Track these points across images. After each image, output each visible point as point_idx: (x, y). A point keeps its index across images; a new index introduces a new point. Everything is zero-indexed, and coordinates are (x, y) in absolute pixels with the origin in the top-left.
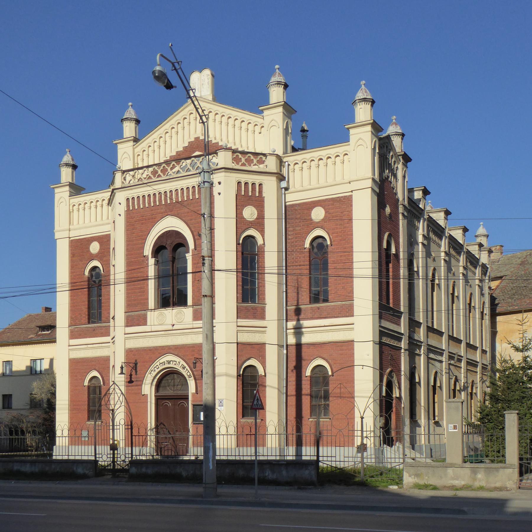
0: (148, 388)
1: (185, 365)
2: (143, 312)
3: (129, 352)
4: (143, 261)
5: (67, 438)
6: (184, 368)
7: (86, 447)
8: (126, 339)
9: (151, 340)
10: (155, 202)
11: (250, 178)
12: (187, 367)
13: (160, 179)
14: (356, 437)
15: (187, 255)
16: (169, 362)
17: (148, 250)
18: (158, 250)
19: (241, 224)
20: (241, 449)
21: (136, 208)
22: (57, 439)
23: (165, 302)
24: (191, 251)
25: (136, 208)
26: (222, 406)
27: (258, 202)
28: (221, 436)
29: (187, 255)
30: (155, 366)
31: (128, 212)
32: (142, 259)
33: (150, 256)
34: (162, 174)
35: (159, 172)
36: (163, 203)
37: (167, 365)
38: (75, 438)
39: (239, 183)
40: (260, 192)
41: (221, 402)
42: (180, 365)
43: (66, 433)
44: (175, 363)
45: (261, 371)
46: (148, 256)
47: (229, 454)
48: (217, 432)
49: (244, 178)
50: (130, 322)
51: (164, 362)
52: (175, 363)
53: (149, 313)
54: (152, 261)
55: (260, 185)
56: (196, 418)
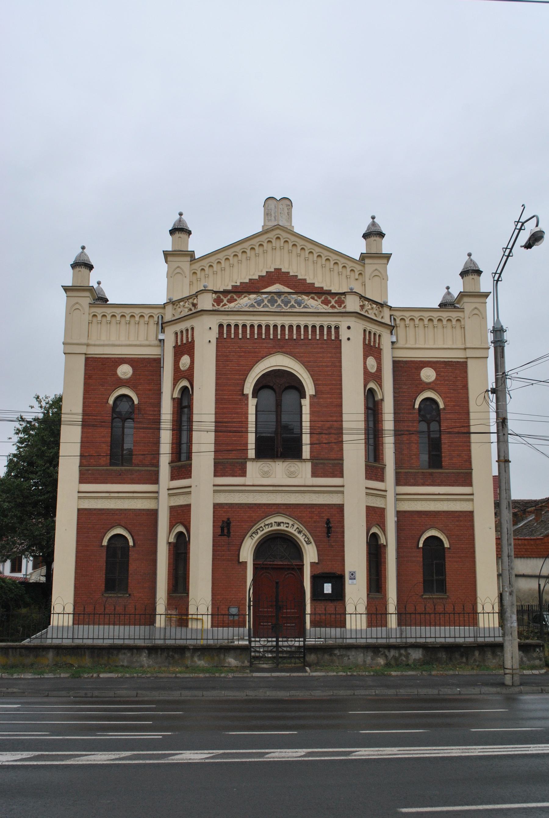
0: (247, 553)
1: (302, 528)
4: (240, 400)
5: (71, 616)
6: (300, 532)
8: (215, 491)
9: (251, 495)
10: (260, 333)
12: (305, 531)
14: (52, 615)
15: (303, 401)
16: (279, 524)
17: (248, 389)
19: (368, 376)
20: (374, 629)
21: (233, 336)
25: (248, 337)
26: (355, 579)
28: (486, 615)
29: (303, 401)
30: (258, 527)
31: (220, 339)
32: (240, 397)
33: (250, 396)
35: (279, 302)
36: (272, 337)
37: (275, 528)
38: (82, 615)
39: (365, 331)
41: (352, 574)
42: (295, 528)
44: (287, 525)
45: (382, 541)
46: (247, 395)
47: (379, 636)
51: (271, 523)
52: (287, 525)
53: (249, 465)
54: (252, 403)
55: (380, 336)
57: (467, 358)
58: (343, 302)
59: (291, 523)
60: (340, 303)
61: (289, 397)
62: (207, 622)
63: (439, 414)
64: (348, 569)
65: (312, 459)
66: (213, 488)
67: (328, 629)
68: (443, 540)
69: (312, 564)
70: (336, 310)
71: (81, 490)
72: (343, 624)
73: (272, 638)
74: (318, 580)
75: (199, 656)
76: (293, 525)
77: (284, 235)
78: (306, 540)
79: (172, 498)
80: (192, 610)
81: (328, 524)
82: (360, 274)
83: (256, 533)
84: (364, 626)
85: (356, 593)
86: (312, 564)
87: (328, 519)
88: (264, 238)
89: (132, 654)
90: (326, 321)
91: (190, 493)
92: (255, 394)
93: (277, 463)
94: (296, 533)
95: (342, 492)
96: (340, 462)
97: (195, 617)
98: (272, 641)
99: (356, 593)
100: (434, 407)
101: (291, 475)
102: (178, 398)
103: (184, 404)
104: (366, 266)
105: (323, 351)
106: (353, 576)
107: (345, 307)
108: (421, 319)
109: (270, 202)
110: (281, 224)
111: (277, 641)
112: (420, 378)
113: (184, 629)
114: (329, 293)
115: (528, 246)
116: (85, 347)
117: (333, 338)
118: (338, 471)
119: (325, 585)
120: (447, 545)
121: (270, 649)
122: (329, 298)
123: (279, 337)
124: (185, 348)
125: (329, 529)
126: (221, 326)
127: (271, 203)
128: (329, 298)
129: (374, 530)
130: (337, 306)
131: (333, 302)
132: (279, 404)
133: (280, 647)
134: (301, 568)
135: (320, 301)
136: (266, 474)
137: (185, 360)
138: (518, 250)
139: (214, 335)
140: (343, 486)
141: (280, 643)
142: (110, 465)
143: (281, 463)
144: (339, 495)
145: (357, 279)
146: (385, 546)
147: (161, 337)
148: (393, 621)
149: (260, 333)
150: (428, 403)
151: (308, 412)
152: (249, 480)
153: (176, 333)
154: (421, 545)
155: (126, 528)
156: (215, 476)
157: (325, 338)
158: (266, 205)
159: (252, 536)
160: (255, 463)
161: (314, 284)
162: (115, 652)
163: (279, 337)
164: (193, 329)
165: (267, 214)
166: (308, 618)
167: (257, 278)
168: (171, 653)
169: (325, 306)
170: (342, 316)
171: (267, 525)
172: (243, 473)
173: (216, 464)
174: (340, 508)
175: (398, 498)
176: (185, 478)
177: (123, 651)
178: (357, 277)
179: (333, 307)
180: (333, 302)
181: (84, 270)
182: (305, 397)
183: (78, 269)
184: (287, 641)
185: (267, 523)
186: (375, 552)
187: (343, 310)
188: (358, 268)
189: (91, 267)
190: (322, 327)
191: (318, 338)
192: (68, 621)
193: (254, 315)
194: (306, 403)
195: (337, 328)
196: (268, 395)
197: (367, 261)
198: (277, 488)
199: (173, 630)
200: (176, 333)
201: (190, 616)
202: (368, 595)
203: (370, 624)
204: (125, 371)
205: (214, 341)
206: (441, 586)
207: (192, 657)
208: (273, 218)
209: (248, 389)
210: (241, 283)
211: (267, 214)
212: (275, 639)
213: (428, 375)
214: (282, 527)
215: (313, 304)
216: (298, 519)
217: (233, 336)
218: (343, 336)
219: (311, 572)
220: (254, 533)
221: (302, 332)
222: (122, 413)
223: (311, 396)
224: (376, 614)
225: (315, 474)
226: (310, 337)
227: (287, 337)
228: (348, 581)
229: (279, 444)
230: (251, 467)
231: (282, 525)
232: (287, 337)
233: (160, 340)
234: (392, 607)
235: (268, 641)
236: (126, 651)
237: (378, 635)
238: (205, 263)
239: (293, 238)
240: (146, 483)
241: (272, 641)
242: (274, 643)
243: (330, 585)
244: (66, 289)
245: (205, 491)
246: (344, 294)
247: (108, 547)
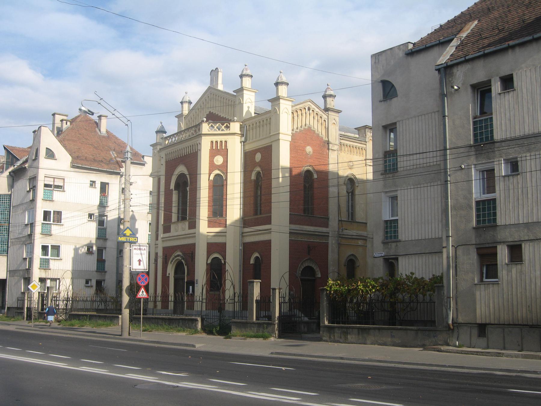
11: (219, 139)
17: (172, 186)
18: (177, 186)
27: (225, 153)
31: (166, 162)
39: (212, 142)
40: (226, 146)
45: (223, 262)
49: (214, 139)
55: (226, 142)
57: (272, 142)
83: (172, 261)
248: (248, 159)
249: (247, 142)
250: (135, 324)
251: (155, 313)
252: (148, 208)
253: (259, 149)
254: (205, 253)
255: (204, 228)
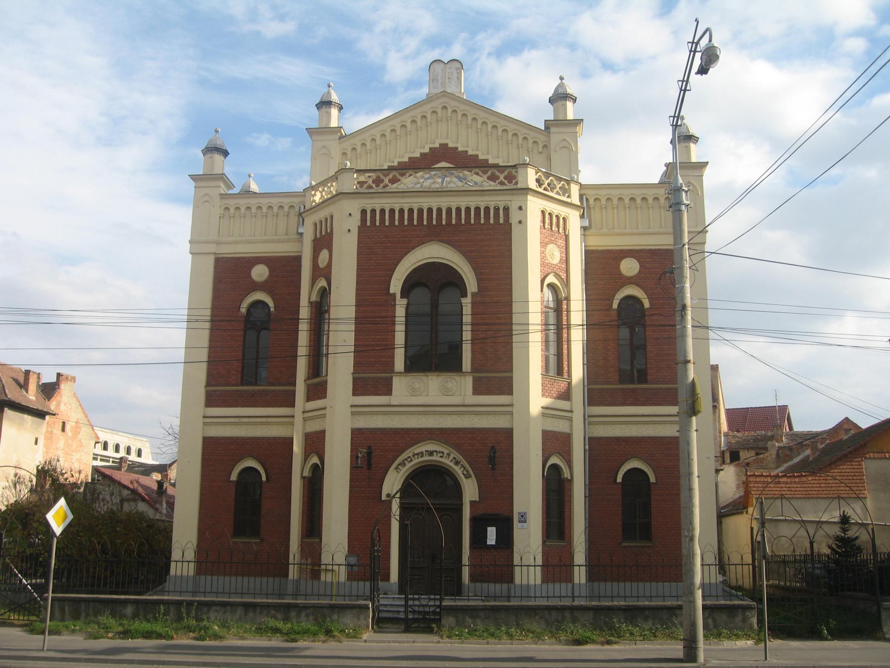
1: (460, 457)
2: (387, 375)
3: (357, 434)
5: (192, 565)
6: (457, 463)
7: (209, 578)
8: (353, 413)
10: (411, 218)
13: (371, 191)
15: (464, 300)
16: (431, 453)
17: (396, 286)
20: (551, 586)
21: (378, 224)
22: (173, 565)
23: (418, 363)
24: (469, 295)
26: (525, 522)
29: (464, 300)
33: (398, 295)
34: (374, 186)
39: (543, 212)
42: (451, 458)
43: (190, 555)
45: (566, 474)
46: (395, 294)
48: (516, 561)
50: (360, 387)
51: (422, 453)
56: (478, 538)
58: (515, 177)
59: (446, 452)
60: (511, 178)
61: (445, 297)
62: (343, 576)
63: (644, 315)
64: (517, 509)
65: (474, 369)
66: (350, 410)
67: (492, 586)
68: (649, 473)
69: (472, 503)
70: (504, 187)
71: (207, 415)
72: (510, 579)
73: (435, 595)
74: (479, 524)
75: (307, 616)
76: (449, 455)
77: (452, 104)
78: (465, 473)
79: (308, 423)
80: (325, 558)
81: (492, 453)
82: (545, 146)
83: (403, 464)
84: (539, 581)
85: (529, 539)
86: (472, 503)
87: (493, 447)
88: (428, 108)
89: (225, 612)
90: (491, 201)
91: (324, 416)
92: (405, 292)
93: (430, 377)
94: (452, 464)
95: (511, 413)
96: (508, 374)
97: (330, 567)
98: (435, 599)
99: (529, 539)
100: (638, 306)
101: (446, 392)
102: (316, 302)
103: (320, 310)
104: (552, 135)
105: (490, 240)
106: (523, 518)
107: (516, 183)
108: (620, 199)
109: (436, 65)
110: (449, 90)
111: (407, 600)
112: (620, 271)
113: (316, 583)
114: (496, 166)
115: (703, 71)
116: (215, 245)
117: (501, 221)
118: (505, 386)
119: (489, 529)
120: (652, 479)
121: (432, 609)
122: (497, 173)
123: (434, 223)
124: (324, 241)
125: (492, 460)
126: (364, 212)
127: (438, 67)
128: (497, 173)
129: (554, 460)
130: (506, 182)
131: (502, 178)
132: (435, 305)
133: (410, 606)
134: (459, 509)
135: (485, 177)
136: (414, 392)
137: (324, 254)
138: (695, 78)
139: (354, 223)
140: (512, 405)
141: (403, 603)
142: (242, 385)
143: (434, 378)
144: (508, 417)
145: (541, 153)
146: (571, 481)
147: (300, 231)
148: (580, 575)
149: (411, 218)
150: (631, 302)
151: (469, 312)
152: (395, 399)
153: (316, 224)
154: (619, 480)
155: (258, 459)
156: (354, 394)
157: (492, 221)
158: (432, 70)
159: (397, 468)
160: (403, 378)
161: (467, 151)
162: (205, 609)
163: (434, 223)
164: (332, 217)
165: (433, 80)
166: (466, 572)
167: (418, 155)
168: (273, 612)
169: (491, 183)
170: (512, 194)
171: (417, 454)
172: (388, 392)
173: (355, 381)
174: (508, 434)
175: (588, 419)
176: (320, 398)
177: (214, 608)
178: (541, 149)
179: (502, 183)
180: (502, 178)
181: (218, 158)
182: (466, 296)
183: (209, 155)
184: (418, 599)
185: (416, 452)
186: (556, 488)
187: (514, 187)
188: (541, 139)
189: (225, 153)
190: (487, 209)
191: (482, 222)
192: (190, 570)
193: (403, 197)
194: (467, 302)
195: (506, 209)
196: (422, 295)
197: (553, 130)
198: (428, 409)
199: (309, 582)
200: (316, 224)
201: (323, 567)
202: (544, 542)
203: (547, 578)
204: (260, 273)
205: (355, 231)
206: (646, 533)
207: (298, 616)
208: (439, 84)
209: (396, 286)
210: (399, 163)
211: (433, 80)
212: (438, 597)
213: (629, 267)
214: (435, 458)
215: (476, 179)
216: (457, 447)
217: (378, 224)
218: (514, 220)
219: (471, 513)
220: (400, 464)
221: (463, 216)
222: (257, 322)
223: (473, 294)
224: (556, 566)
225: (477, 391)
226: (472, 222)
227: (444, 223)
228: (516, 525)
229: (434, 355)
230: (399, 384)
231: (435, 454)
232: (444, 223)
233: (298, 233)
234: (580, 556)
235: (430, 599)
236: (218, 608)
237: (558, 595)
238: (357, 141)
239: (463, 107)
240: (279, 406)
241: (435, 599)
242: (438, 603)
243: (494, 528)
244: (194, 178)
245: (341, 414)
246: (514, 166)
247: (237, 483)
248: (601, 266)
249: (593, 230)
250: (460, 624)
251: (576, 593)
252: (185, 325)
253: (631, 251)
254: (540, 453)
255: (537, 399)
